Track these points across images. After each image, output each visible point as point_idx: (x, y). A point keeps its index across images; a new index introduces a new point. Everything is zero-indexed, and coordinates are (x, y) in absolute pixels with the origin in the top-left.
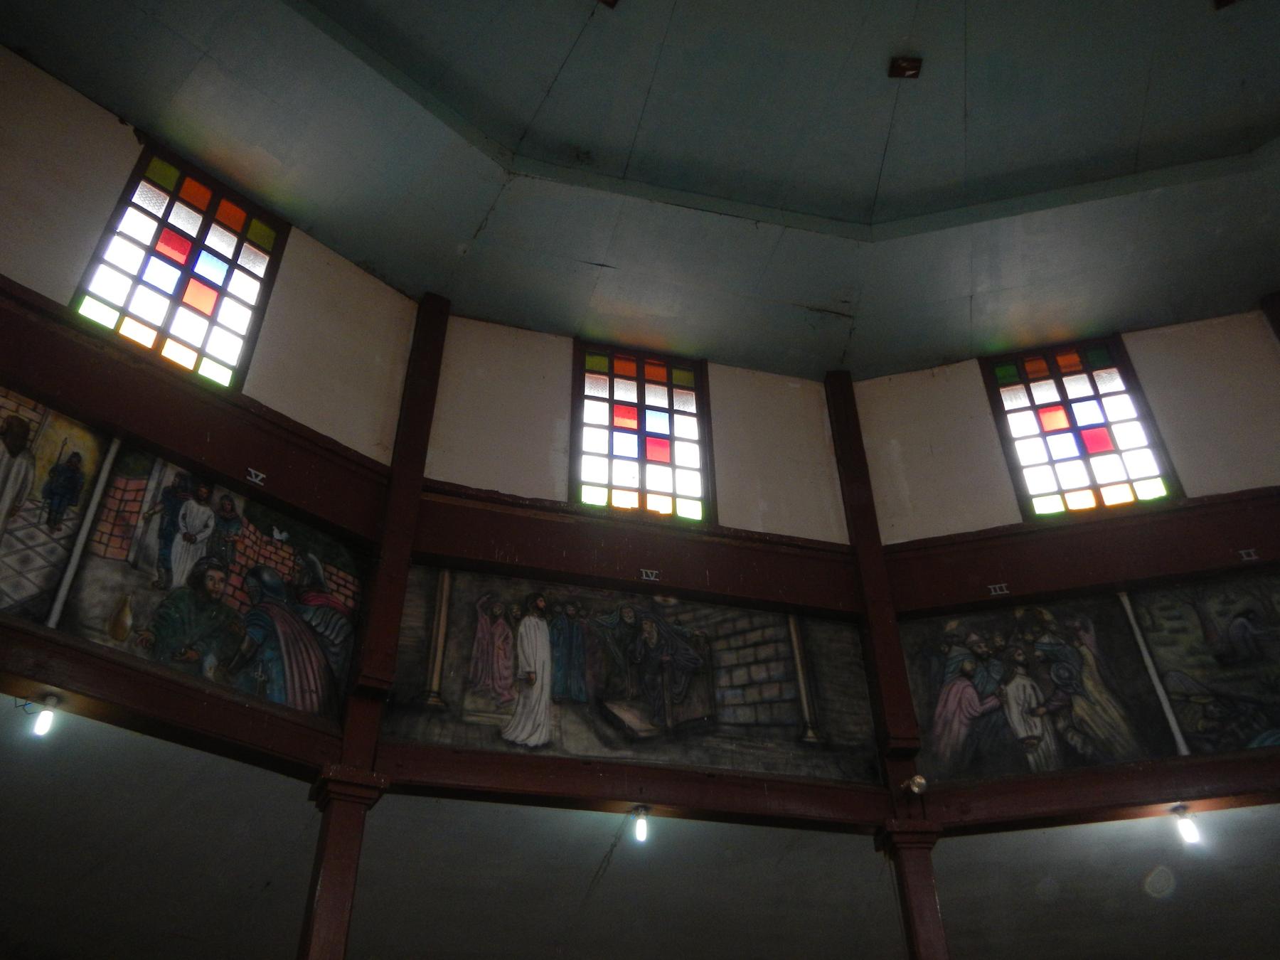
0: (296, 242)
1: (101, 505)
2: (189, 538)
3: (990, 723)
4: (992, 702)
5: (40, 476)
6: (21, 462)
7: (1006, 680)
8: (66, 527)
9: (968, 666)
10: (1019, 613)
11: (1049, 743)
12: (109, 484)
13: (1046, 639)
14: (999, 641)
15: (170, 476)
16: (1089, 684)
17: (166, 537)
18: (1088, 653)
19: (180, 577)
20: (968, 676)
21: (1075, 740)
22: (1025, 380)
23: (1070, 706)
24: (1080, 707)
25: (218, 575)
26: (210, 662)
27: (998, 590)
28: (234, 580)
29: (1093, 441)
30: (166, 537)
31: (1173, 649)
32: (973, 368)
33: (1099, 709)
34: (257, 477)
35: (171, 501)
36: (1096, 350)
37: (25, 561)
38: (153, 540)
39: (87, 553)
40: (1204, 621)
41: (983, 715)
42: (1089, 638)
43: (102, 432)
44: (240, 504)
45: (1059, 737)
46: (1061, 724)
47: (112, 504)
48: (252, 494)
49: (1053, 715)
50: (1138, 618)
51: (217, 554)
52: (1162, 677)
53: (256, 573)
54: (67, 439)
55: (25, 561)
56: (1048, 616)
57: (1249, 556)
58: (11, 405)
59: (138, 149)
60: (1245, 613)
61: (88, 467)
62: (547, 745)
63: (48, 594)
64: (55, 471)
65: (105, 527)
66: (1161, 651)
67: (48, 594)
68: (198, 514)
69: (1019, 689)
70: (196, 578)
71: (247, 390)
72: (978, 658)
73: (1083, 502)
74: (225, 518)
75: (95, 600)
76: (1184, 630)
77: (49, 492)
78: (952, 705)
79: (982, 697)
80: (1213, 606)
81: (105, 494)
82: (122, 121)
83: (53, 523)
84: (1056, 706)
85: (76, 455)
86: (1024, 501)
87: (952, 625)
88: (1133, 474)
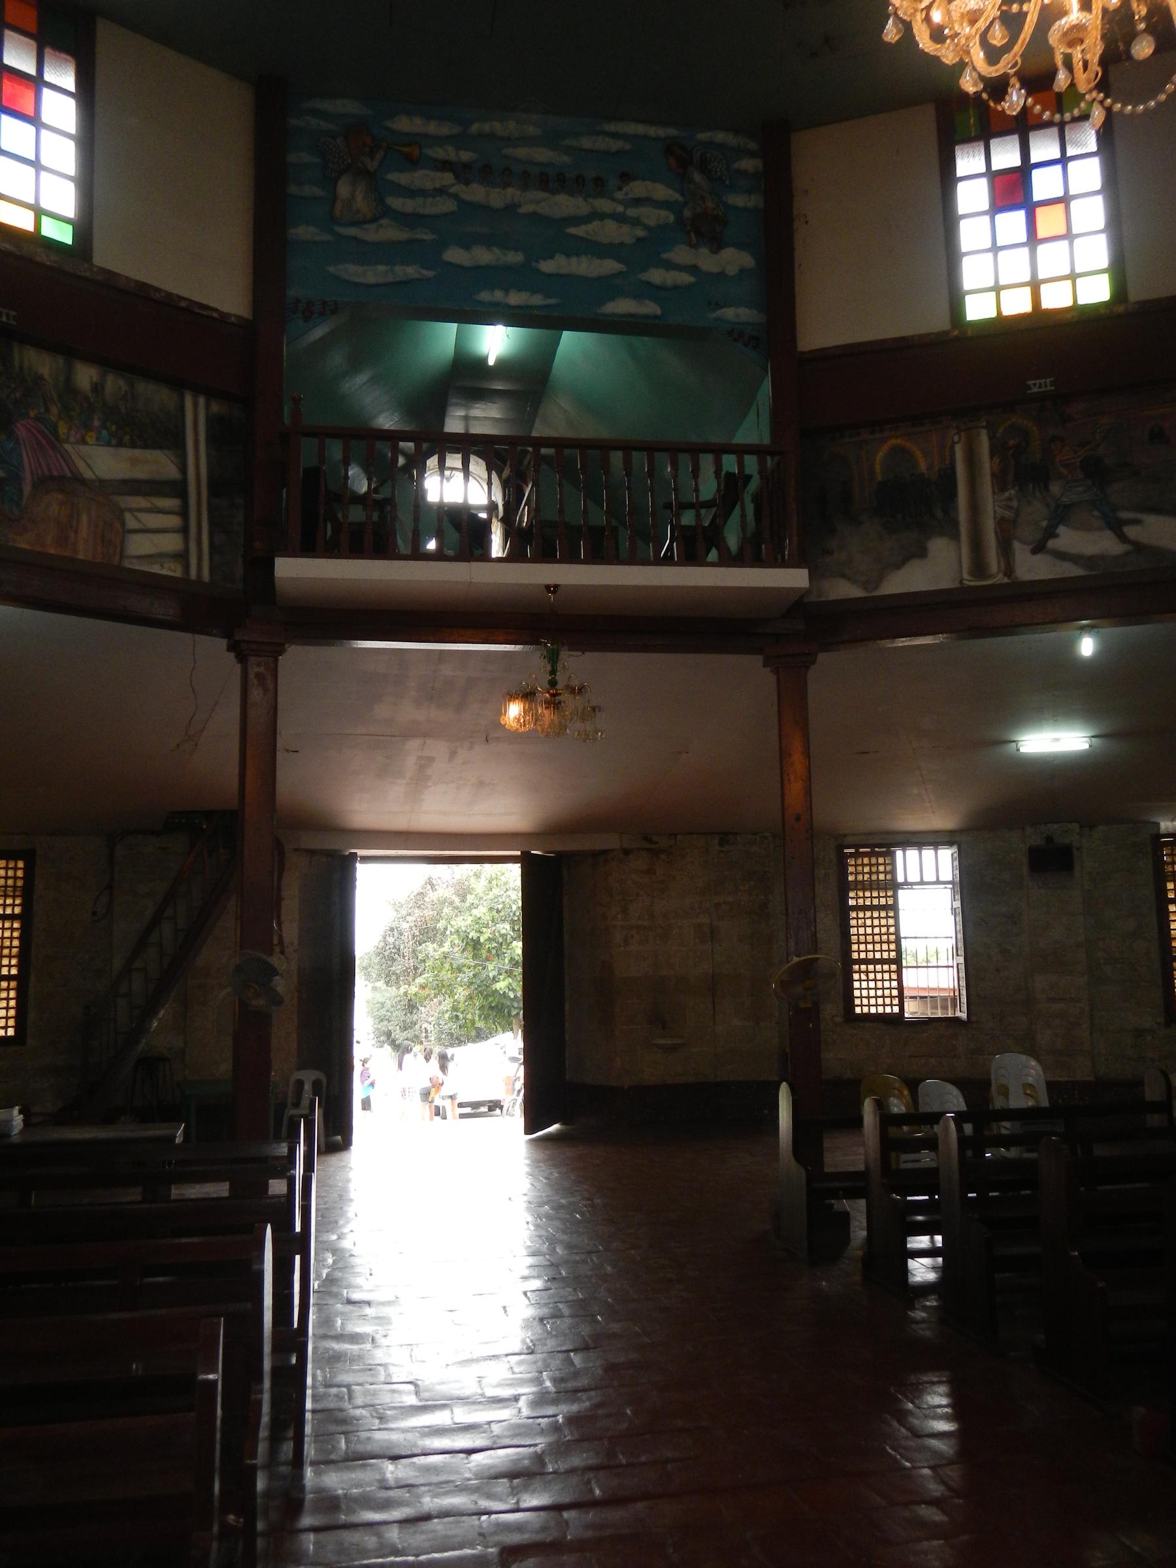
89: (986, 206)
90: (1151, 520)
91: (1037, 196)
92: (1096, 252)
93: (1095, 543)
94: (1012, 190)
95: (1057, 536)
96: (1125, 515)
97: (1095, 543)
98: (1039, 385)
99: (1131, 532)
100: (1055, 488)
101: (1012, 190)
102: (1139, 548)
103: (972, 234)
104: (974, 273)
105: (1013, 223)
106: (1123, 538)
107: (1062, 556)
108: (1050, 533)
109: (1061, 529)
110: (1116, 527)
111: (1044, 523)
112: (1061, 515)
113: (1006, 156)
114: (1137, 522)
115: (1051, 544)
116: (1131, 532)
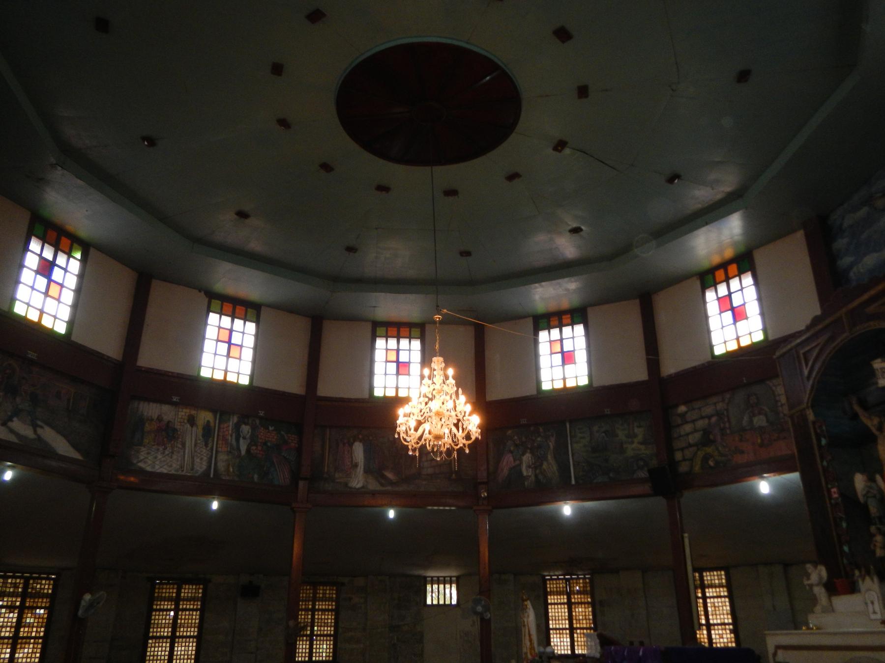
0: (264, 310)
1: (218, 435)
2: (244, 438)
3: (516, 471)
4: (518, 462)
5: (200, 431)
6: (194, 429)
7: (523, 454)
8: (210, 445)
9: (512, 448)
10: (532, 428)
11: (533, 478)
12: (219, 428)
13: (539, 439)
14: (524, 439)
15: (235, 419)
16: (549, 457)
17: (238, 440)
18: (551, 445)
19: (243, 452)
20: (511, 452)
21: (541, 477)
22: (549, 328)
23: (541, 465)
24: (545, 466)
25: (254, 448)
26: (256, 476)
27: (524, 421)
28: (260, 448)
29: (567, 358)
30: (238, 440)
31: (578, 445)
32: (530, 321)
33: (551, 466)
34: (261, 413)
35: (237, 427)
37: (201, 459)
38: (234, 442)
39: (217, 451)
41: (514, 467)
42: (553, 439)
43: (214, 412)
44: (258, 422)
45: (536, 476)
46: (538, 471)
47: (221, 434)
48: (261, 418)
49: (536, 468)
51: (253, 441)
53: (265, 444)
54: (205, 417)
55: (201, 459)
56: (541, 430)
57: (607, 411)
58: (188, 411)
59: (207, 300)
60: (604, 432)
61: (212, 424)
62: (363, 487)
63: (209, 467)
64: (204, 429)
65: (220, 442)
66: (575, 445)
67: (209, 467)
68: (246, 429)
69: (527, 458)
70: (248, 451)
71: (255, 384)
72: (516, 446)
74: (254, 428)
75: (221, 466)
76: (583, 438)
77: (203, 436)
78: (504, 463)
79: (515, 461)
80: (596, 428)
81: (218, 431)
82: (200, 291)
83: (206, 445)
84: (536, 466)
85: (208, 422)
86: (539, 383)
87: (509, 432)
88: (578, 375)
89: (35, 268)
90: (48, 430)
91: (54, 278)
92: (65, 313)
93: (26, 431)
94: (46, 268)
95: (12, 421)
96: (39, 423)
97: (26, 431)
98: (32, 355)
99: (39, 431)
100: (18, 400)
101: (46, 268)
102: (39, 439)
103: (27, 276)
104: (22, 292)
105: (42, 282)
106: (35, 431)
107: (12, 431)
108: (10, 419)
109: (15, 419)
110: (35, 426)
111: (9, 414)
112: (17, 413)
113: (48, 254)
114: (42, 427)
115: (10, 424)
116: (39, 431)
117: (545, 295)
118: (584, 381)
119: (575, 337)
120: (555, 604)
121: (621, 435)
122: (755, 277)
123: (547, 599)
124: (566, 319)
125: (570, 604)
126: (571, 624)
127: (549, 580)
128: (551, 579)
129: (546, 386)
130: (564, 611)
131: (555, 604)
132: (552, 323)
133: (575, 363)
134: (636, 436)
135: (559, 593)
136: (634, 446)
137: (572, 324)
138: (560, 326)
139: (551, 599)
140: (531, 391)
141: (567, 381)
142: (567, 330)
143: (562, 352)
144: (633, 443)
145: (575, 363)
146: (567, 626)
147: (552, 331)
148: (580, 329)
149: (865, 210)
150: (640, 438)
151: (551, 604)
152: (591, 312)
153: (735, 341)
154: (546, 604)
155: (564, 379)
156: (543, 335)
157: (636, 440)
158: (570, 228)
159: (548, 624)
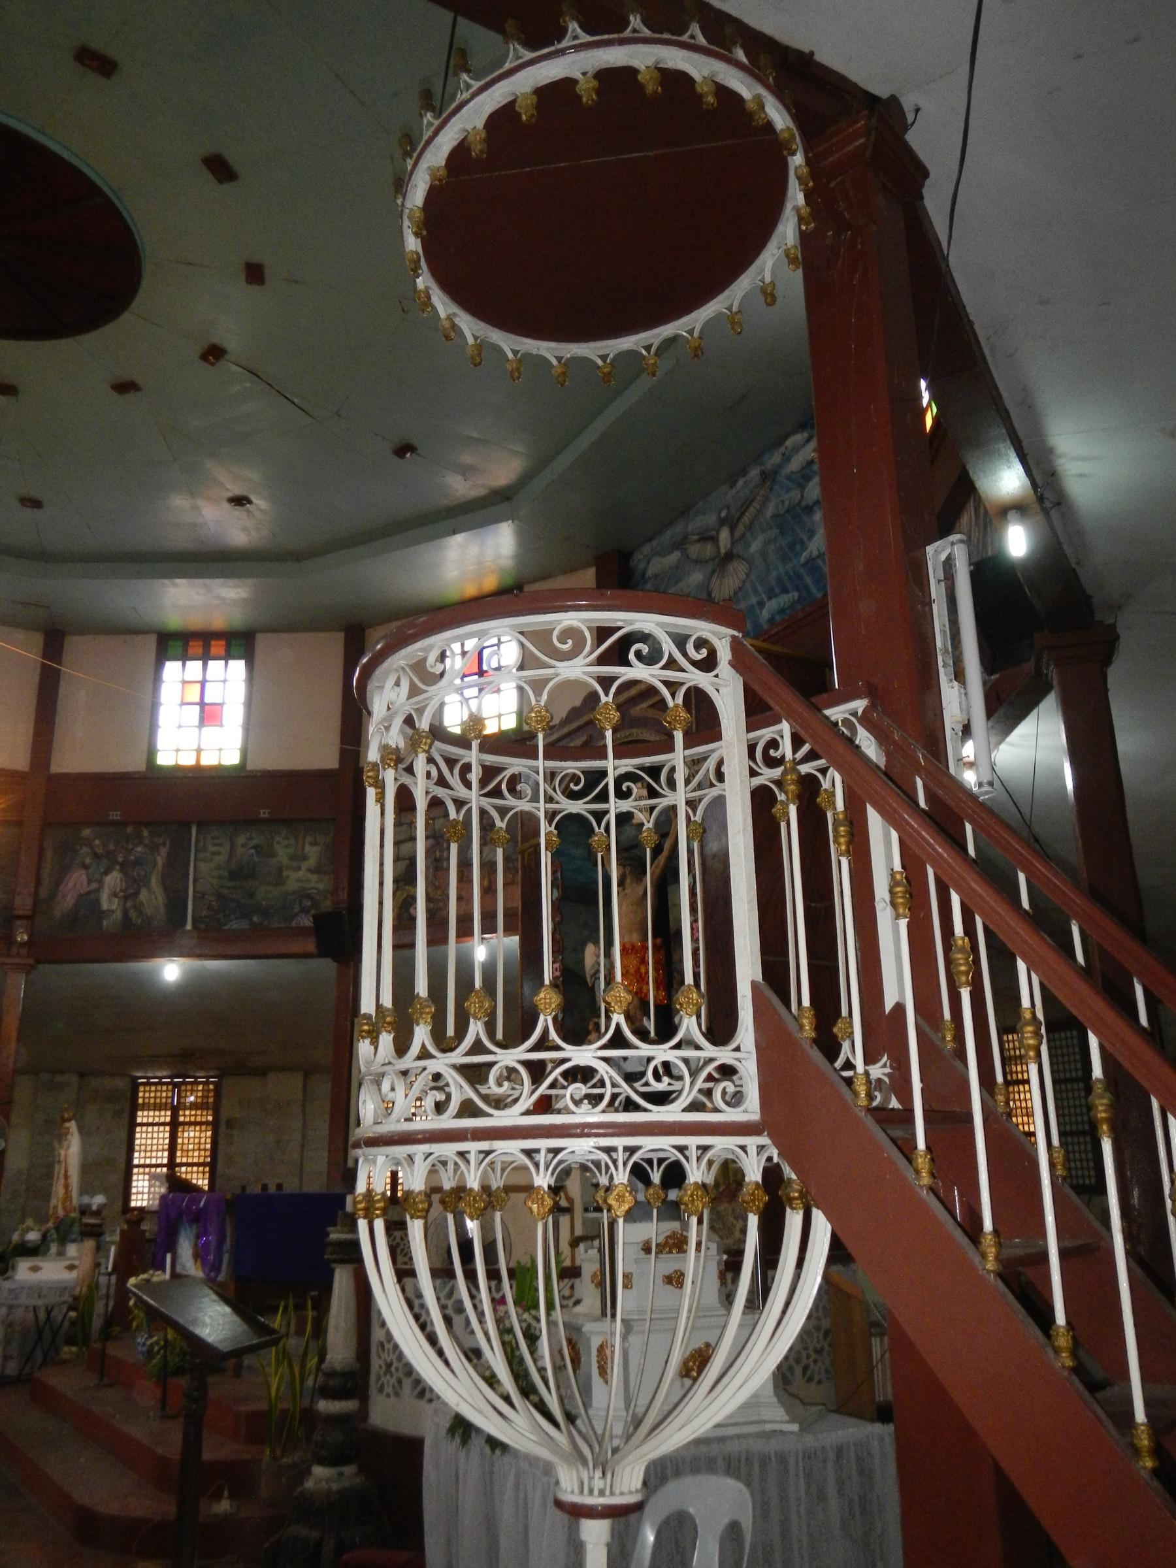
3: (89, 901)
4: (94, 886)
7: (106, 873)
9: (88, 861)
10: (130, 829)
11: (118, 915)
13: (139, 849)
14: (112, 847)
16: (154, 881)
18: (160, 861)
20: (85, 867)
21: (133, 914)
22: (184, 657)
23: (136, 894)
24: (143, 895)
27: (115, 815)
29: (208, 714)
31: (207, 865)
32: (152, 640)
33: (153, 898)
36: (236, 642)
40: (233, 847)
41: (89, 893)
42: (164, 851)
45: (125, 913)
46: (129, 904)
49: (126, 898)
50: (197, 840)
52: (195, 881)
56: (146, 833)
57: (264, 814)
60: (255, 847)
66: (203, 866)
69: (113, 879)
72: (96, 856)
73: (188, 760)
76: (219, 853)
78: (70, 885)
79: (90, 881)
80: (241, 840)
84: (129, 895)
86: (152, 752)
87: (87, 832)
88: (223, 747)
117: (184, 600)
118: (232, 758)
119: (229, 680)
120: (148, 1124)
121: (283, 854)
122: (250, 667)
123: (133, 1116)
124: (217, 647)
125: (175, 1126)
126: (172, 1156)
127: (143, 1084)
128: (149, 1084)
129: (165, 759)
130: (164, 1135)
131: (148, 1124)
132: (191, 651)
133: (221, 725)
134: (305, 858)
135: (157, 1107)
136: (300, 874)
137: (227, 656)
138: (205, 657)
139: (142, 1116)
140: (134, 764)
141: (203, 753)
142: (216, 666)
143: (202, 704)
144: (299, 869)
145: (221, 725)
146: (165, 1161)
147: (190, 664)
148: (238, 667)
149: (676, 556)
150: (312, 862)
151: (142, 1125)
152: (261, 641)
153: (194, 754)
154: (133, 1125)
155: (199, 751)
156: (172, 669)
157: (305, 866)
158: (230, 494)
159: (130, 1158)
